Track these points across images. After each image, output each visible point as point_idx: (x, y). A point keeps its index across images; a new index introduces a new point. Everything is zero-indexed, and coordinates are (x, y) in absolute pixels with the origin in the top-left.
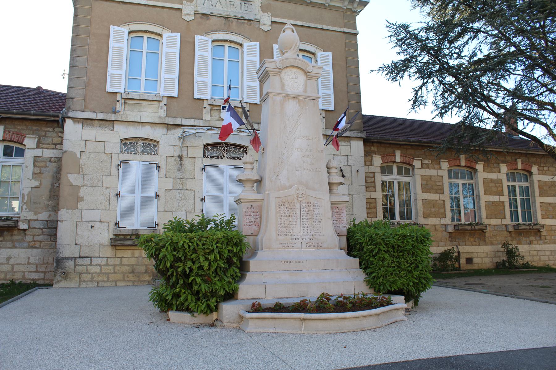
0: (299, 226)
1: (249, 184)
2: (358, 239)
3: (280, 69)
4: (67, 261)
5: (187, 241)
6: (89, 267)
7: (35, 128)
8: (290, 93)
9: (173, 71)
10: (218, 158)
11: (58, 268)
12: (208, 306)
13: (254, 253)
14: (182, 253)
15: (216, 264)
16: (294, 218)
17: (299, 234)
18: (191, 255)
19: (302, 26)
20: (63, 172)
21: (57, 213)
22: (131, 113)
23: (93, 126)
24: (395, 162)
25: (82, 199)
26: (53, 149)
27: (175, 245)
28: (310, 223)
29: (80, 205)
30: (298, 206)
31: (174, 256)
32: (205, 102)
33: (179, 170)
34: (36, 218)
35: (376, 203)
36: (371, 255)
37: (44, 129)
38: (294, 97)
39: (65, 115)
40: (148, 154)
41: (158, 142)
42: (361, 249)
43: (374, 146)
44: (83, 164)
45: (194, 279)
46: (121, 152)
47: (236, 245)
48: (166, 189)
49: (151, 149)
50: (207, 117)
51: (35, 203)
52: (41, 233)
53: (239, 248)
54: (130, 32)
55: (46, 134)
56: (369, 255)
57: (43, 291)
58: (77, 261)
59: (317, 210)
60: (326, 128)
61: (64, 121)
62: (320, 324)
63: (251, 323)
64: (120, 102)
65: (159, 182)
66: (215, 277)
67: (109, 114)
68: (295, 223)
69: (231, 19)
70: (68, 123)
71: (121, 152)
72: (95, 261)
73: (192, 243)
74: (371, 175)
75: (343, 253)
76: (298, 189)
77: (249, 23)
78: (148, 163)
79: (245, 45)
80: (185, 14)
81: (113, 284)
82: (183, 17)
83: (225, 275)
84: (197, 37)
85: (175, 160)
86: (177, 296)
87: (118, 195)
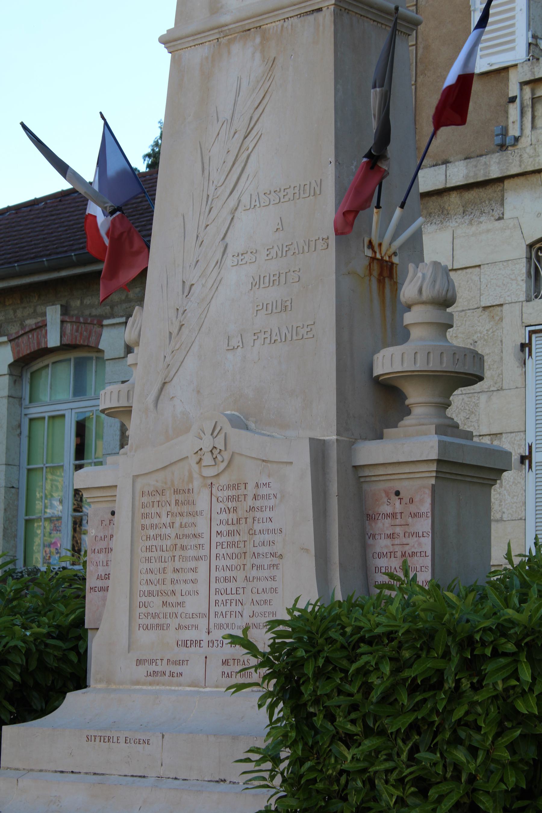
0: (203, 588)
16: (191, 553)
17: (203, 623)
23: (445, 214)
28: (240, 575)
30: (202, 502)
59: (268, 514)
67: (483, 159)
68: (190, 576)
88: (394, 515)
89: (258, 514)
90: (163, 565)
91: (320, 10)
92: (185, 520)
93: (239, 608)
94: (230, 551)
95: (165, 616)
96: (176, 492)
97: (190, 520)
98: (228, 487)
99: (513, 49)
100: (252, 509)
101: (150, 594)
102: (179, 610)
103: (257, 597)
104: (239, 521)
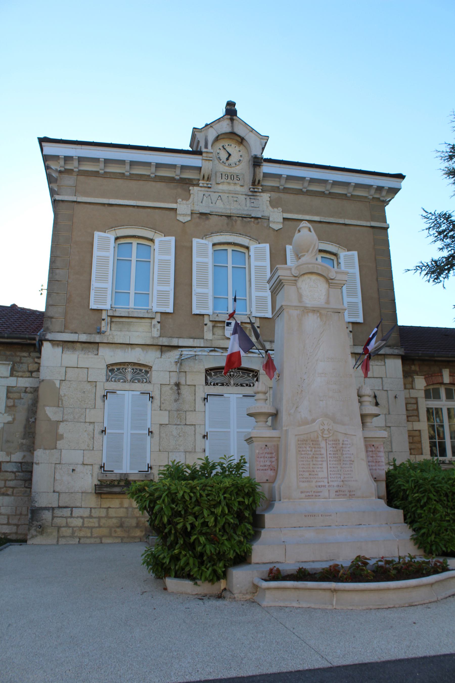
0: (325, 470)
1: (262, 419)
2: (400, 485)
3: (295, 277)
4: (44, 511)
5: (188, 491)
6: (69, 520)
7: (8, 353)
8: (309, 306)
9: (168, 282)
10: (223, 385)
11: (33, 521)
12: (215, 572)
13: (270, 504)
14: (181, 506)
15: (224, 519)
16: (319, 459)
17: (326, 480)
18: (193, 508)
19: (320, 222)
20: (40, 404)
21: (33, 454)
22: (119, 333)
23: (74, 349)
24: (442, 383)
25: (61, 437)
26: (29, 377)
27: (174, 496)
29: (60, 444)
30: (323, 444)
31: (172, 509)
32: (206, 318)
33: (176, 401)
34: (8, 459)
35: (420, 436)
36: (419, 505)
37: (18, 354)
38: (315, 310)
39: (43, 338)
40: (139, 381)
41: (150, 367)
42: (405, 498)
43: (414, 365)
44: (63, 395)
45: (197, 539)
46: (107, 380)
47: (248, 495)
48: (161, 425)
49: (143, 376)
50: (208, 335)
51: (7, 441)
52: (13, 478)
53: (251, 499)
54: (117, 239)
55: (20, 360)
56: (416, 506)
57: (15, 548)
58: (55, 511)
59: (347, 449)
60: (354, 345)
61: (41, 345)
62: (356, 597)
63: (268, 594)
64: (106, 320)
65: (153, 416)
66: (223, 536)
67: (93, 335)
69: (234, 218)
70: (47, 347)
71: (107, 380)
72: (76, 512)
73: (194, 493)
74: (413, 401)
75: (382, 503)
76: (323, 424)
77: (256, 221)
78: (139, 393)
79: (252, 248)
80: (180, 215)
81: (98, 540)
82: (178, 218)
83: (235, 533)
84: (195, 241)
85: (171, 389)
86: (175, 559)
87: (104, 431)
88: (372, 451)
89: (344, 449)
90: (309, 463)
91: (340, 312)
92: (316, 450)
93: (339, 476)
94: (335, 459)
95: (311, 478)
96: (312, 441)
97: (318, 449)
98: (333, 441)
99: (106, 305)
100: (342, 447)
101: (303, 471)
102: (317, 476)
103: (345, 473)
104: (337, 451)
